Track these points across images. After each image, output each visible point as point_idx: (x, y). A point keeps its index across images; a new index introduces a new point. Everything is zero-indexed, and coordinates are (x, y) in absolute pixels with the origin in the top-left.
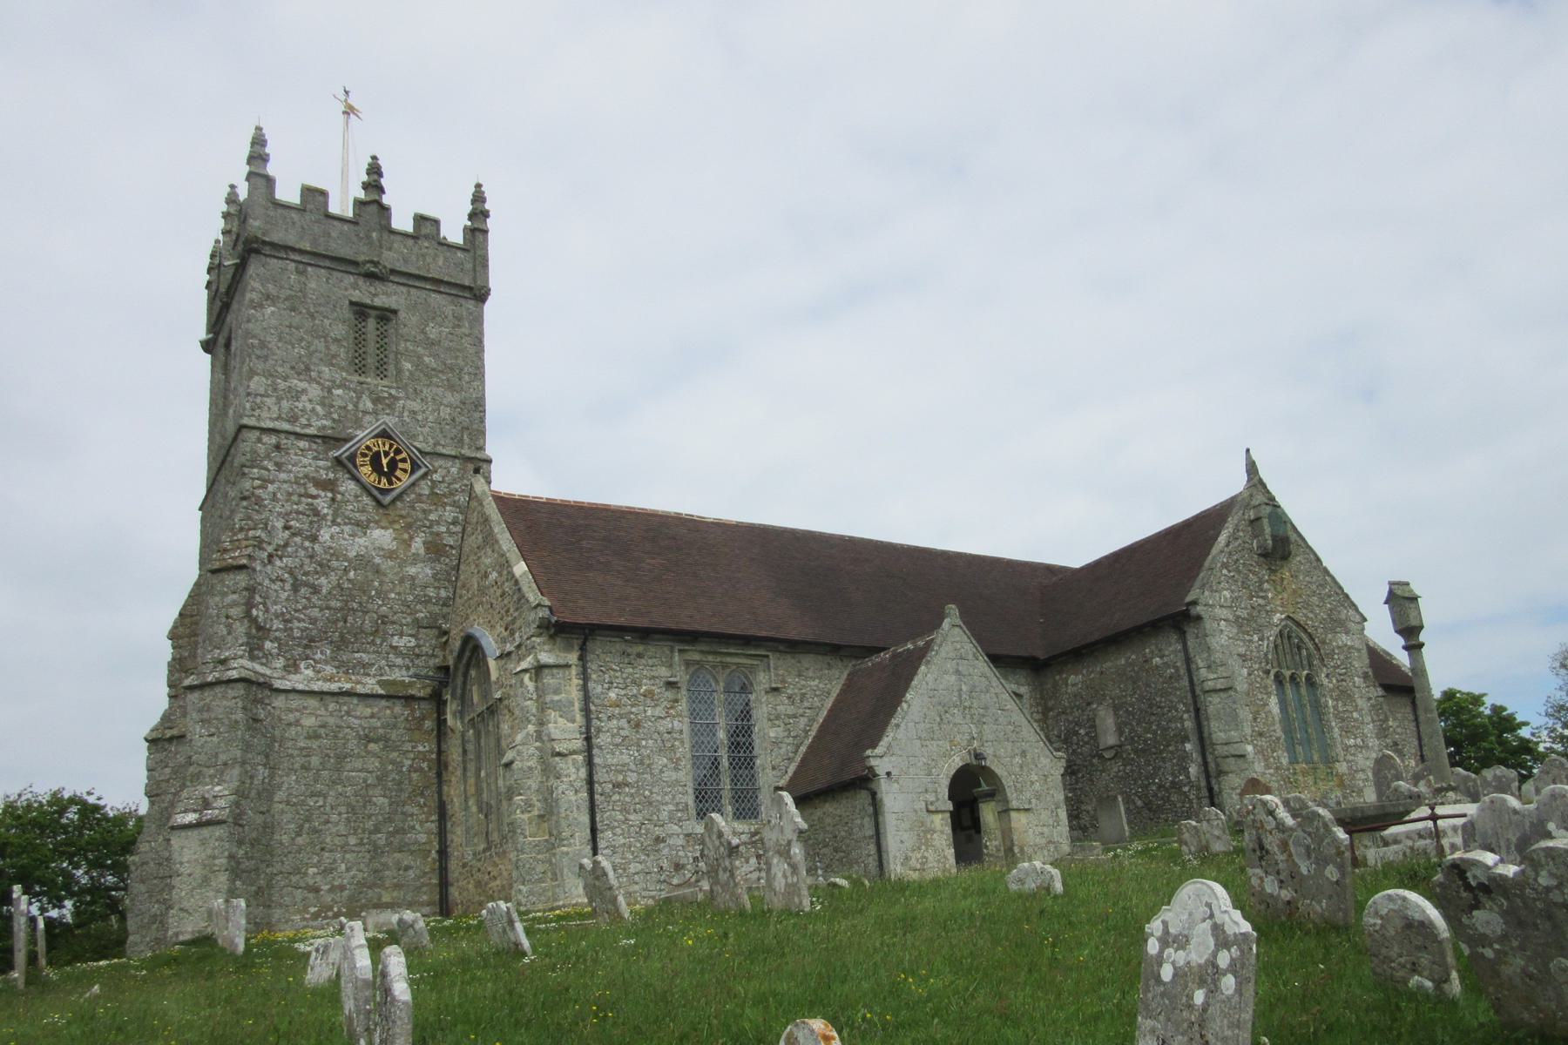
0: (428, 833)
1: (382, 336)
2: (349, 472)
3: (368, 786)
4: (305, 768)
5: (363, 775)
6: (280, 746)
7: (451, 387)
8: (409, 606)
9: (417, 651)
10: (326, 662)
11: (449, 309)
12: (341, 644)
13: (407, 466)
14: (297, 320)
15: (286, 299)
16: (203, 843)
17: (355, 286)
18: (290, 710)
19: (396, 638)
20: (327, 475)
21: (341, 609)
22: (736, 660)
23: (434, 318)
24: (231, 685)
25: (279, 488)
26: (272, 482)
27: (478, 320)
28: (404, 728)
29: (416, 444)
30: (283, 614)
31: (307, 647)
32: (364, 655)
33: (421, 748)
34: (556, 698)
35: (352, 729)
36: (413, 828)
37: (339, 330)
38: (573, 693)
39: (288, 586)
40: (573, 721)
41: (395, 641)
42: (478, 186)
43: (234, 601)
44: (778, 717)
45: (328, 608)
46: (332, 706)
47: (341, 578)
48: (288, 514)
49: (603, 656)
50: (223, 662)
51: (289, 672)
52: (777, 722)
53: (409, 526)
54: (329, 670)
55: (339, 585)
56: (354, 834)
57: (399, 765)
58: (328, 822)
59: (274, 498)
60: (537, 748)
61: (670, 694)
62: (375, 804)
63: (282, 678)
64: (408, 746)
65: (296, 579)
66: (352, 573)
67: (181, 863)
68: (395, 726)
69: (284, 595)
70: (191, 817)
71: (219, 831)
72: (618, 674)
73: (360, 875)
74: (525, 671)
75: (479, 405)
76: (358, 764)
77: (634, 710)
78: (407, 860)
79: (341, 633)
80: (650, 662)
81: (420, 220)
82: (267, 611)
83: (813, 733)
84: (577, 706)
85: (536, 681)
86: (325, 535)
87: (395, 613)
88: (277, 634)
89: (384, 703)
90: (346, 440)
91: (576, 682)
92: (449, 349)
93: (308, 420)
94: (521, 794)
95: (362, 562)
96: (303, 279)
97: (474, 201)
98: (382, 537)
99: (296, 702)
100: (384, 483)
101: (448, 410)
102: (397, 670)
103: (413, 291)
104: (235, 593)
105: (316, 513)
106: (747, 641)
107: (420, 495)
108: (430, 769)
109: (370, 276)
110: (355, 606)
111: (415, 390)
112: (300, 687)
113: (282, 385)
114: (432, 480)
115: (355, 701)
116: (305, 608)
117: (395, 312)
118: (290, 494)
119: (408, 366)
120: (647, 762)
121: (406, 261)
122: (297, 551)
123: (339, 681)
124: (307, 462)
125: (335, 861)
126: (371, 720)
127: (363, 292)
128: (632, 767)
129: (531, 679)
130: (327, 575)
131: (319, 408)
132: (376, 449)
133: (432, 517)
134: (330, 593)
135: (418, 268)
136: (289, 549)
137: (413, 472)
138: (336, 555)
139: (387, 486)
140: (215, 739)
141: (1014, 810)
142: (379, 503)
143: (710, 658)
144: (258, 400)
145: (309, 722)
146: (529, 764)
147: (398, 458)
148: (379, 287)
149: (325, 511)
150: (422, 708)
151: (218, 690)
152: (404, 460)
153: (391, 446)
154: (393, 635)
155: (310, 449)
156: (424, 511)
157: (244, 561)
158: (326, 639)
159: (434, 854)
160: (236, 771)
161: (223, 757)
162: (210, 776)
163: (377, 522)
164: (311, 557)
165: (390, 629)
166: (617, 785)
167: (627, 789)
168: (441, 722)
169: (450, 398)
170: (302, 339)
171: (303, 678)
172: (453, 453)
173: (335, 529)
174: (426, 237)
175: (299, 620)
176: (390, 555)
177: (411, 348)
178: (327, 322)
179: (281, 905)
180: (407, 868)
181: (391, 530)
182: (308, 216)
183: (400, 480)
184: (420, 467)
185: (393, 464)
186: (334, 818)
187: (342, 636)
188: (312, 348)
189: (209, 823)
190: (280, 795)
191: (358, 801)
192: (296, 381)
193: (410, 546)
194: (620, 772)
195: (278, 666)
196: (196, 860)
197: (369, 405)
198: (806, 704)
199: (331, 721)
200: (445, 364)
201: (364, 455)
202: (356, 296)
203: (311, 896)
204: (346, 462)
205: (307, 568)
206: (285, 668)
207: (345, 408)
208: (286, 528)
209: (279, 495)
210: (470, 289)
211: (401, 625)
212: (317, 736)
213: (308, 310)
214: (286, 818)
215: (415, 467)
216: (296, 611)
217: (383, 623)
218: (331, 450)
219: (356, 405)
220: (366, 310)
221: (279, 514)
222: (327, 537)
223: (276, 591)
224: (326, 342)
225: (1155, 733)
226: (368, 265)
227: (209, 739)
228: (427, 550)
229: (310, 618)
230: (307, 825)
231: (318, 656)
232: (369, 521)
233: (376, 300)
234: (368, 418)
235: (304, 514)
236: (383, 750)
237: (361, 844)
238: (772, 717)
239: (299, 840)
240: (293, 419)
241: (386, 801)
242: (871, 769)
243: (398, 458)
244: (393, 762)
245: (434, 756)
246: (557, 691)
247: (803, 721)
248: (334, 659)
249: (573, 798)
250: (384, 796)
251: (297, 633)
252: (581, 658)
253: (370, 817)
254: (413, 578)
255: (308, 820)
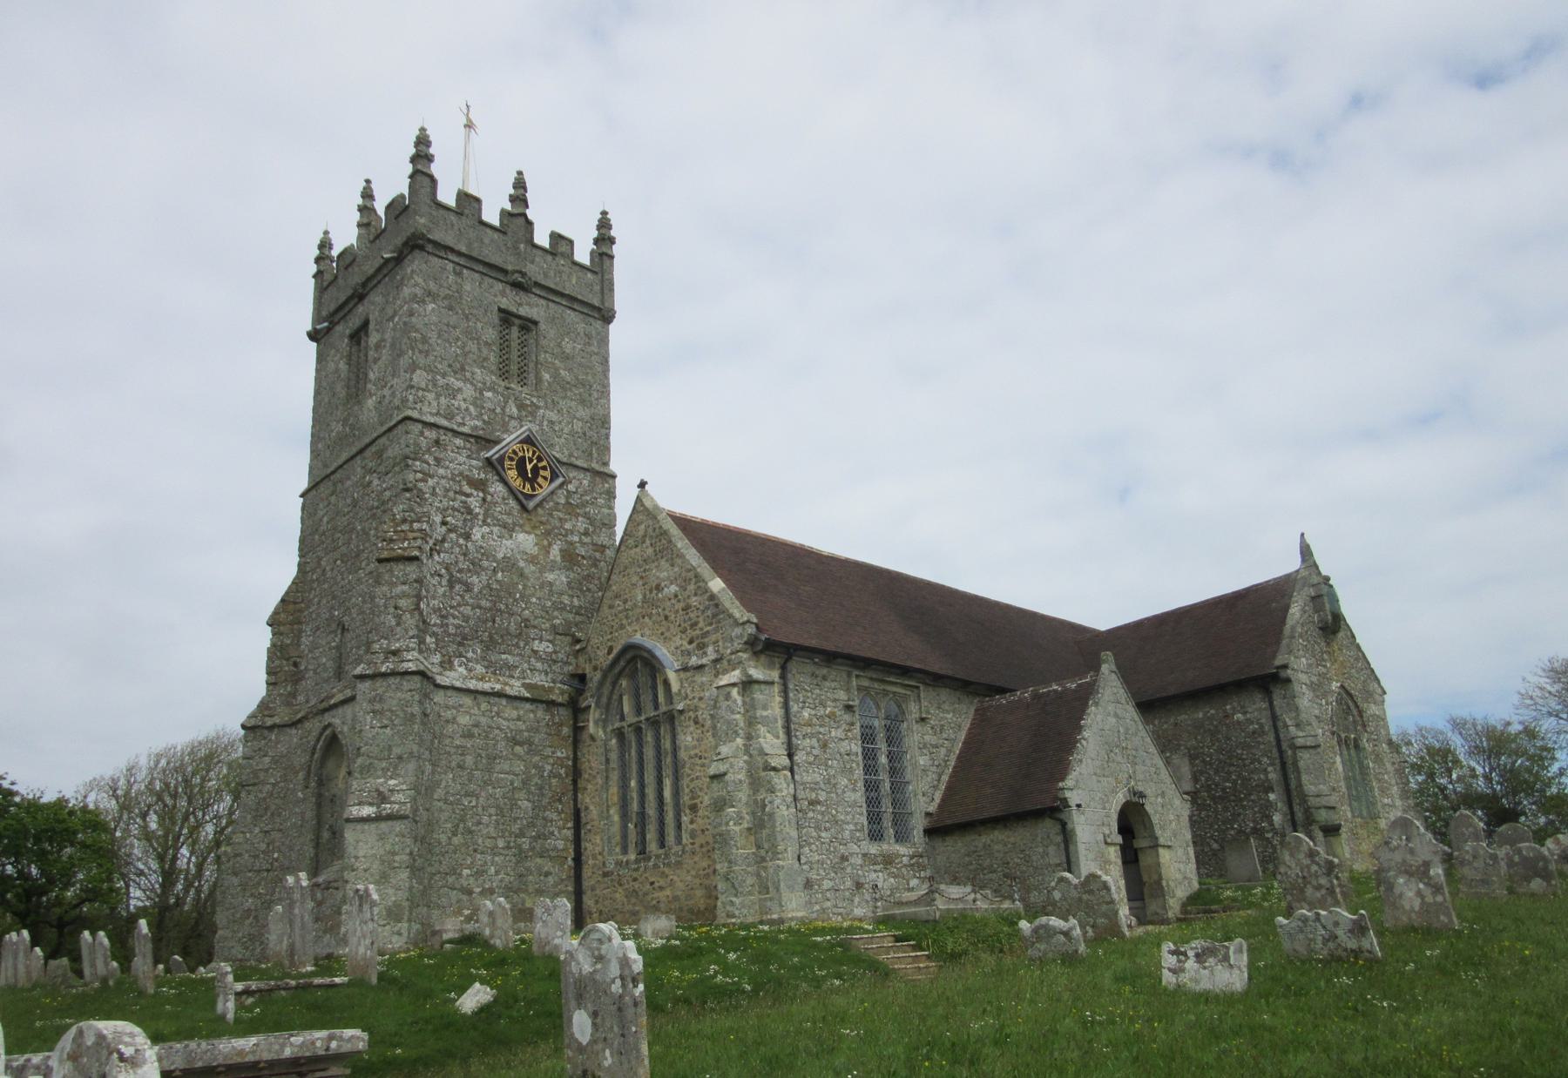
0: (566, 839)
1: (523, 344)
2: (498, 474)
3: (514, 788)
4: (460, 767)
5: (511, 777)
6: (439, 742)
7: (582, 402)
8: (547, 612)
9: (554, 656)
10: (477, 662)
11: (581, 327)
12: (490, 645)
13: (547, 474)
14: (453, 320)
15: (445, 298)
16: (381, 837)
17: (503, 294)
18: (448, 707)
19: (537, 642)
20: (479, 474)
21: (490, 609)
22: (894, 689)
23: (569, 333)
24: (408, 677)
25: (438, 483)
26: (432, 477)
27: (604, 341)
28: (546, 733)
29: (554, 453)
30: (440, 609)
31: (460, 644)
32: (509, 657)
33: (559, 754)
34: (765, 713)
35: (501, 730)
36: (552, 833)
37: (491, 334)
38: (776, 710)
39: (444, 582)
40: (778, 737)
41: (536, 645)
42: (604, 213)
43: (404, 592)
44: (925, 746)
45: (480, 608)
46: (484, 706)
47: (490, 578)
48: (446, 510)
49: (798, 676)
50: (395, 653)
51: (445, 669)
52: (924, 751)
53: (548, 533)
54: (480, 669)
55: (489, 586)
56: (503, 837)
57: (541, 769)
58: (479, 823)
59: (434, 494)
60: (745, 762)
61: (847, 717)
62: (520, 808)
63: (441, 674)
64: (548, 751)
65: (451, 576)
66: (500, 574)
67: (356, 858)
68: (537, 730)
69: (441, 591)
70: (367, 811)
71: (399, 826)
72: (809, 694)
73: (507, 878)
74: (734, 685)
75: (605, 422)
76: (506, 767)
77: (822, 730)
78: (548, 866)
79: (490, 633)
80: (833, 685)
81: (556, 238)
82: (428, 605)
83: (952, 763)
84: (780, 723)
85: (743, 696)
86: (477, 533)
87: (536, 618)
88: (434, 629)
89: (528, 706)
90: (497, 442)
91: (778, 699)
92: (580, 365)
93: (463, 418)
94: (733, 806)
95: (509, 564)
96: (459, 281)
97: (599, 227)
98: (525, 541)
99: (454, 699)
100: (527, 490)
101: (580, 424)
102: (537, 674)
104: (404, 583)
105: (469, 511)
106: (905, 671)
107: (558, 504)
108: (567, 775)
109: (517, 286)
110: (503, 607)
111: (553, 401)
112: (458, 684)
113: (441, 381)
114: (568, 491)
115: (504, 702)
116: (459, 605)
117: (536, 323)
118: (447, 490)
119: (546, 376)
120: (833, 781)
121: (546, 275)
122: (452, 548)
123: (489, 681)
124: (461, 460)
125: (486, 862)
126: (519, 723)
127: (509, 300)
128: (822, 786)
129: (739, 693)
130: (478, 574)
131: (472, 408)
132: (521, 454)
133: (568, 526)
134: (480, 592)
135: (556, 284)
136: (446, 545)
137: (552, 480)
138: (487, 555)
139: (530, 492)
140: (388, 731)
141: (1164, 846)
142: (524, 508)
143: (876, 686)
144: (420, 393)
145: (464, 720)
146: (739, 777)
147: (540, 465)
148: (523, 297)
149: (477, 510)
150: (564, 713)
151: (392, 680)
152: (544, 468)
153: (534, 453)
154: (534, 639)
155: (464, 448)
156: (560, 519)
157: (416, 553)
158: (477, 638)
159: (570, 862)
160: (412, 766)
161: (397, 751)
162: (383, 769)
163: (521, 526)
164: (465, 555)
165: (533, 633)
166: (812, 803)
167: (819, 807)
168: (577, 730)
169: (582, 413)
170: (458, 339)
171: (455, 676)
172: (585, 466)
173: (486, 529)
174: (562, 255)
175: (454, 617)
176: (532, 560)
178: (479, 325)
179: (439, 906)
180: (547, 874)
181: (533, 536)
183: (541, 487)
184: (558, 476)
185: (536, 470)
186: (485, 819)
187: (491, 637)
188: (467, 349)
189: (390, 817)
190: (439, 793)
191: (505, 804)
192: (452, 379)
193: (549, 552)
194: (812, 790)
195: (435, 661)
196: (374, 855)
197: (515, 410)
198: (945, 736)
199: (483, 720)
200: (577, 379)
201: (511, 459)
202: (505, 303)
203: (465, 898)
204: (496, 463)
205: (461, 566)
206: (441, 664)
207: (494, 410)
208: (444, 523)
209: (437, 490)
210: (599, 310)
211: (541, 630)
212: (470, 735)
213: (463, 310)
214: (444, 816)
215: (554, 476)
216: (452, 607)
217: (526, 626)
218: (482, 450)
219: (503, 409)
220: (513, 319)
221: (438, 508)
222: (479, 536)
223: (434, 585)
224: (478, 343)
225: (1234, 782)
226: (516, 275)
227: (381, 731)
228: (563, 557)
229: (463, 616)
230: (461, 826)
231: (470, 655)
232: (514, 524)
233: (520, 309)
234: (513, 423)
235: (459, 511)
236: (528, 753)
237: (508, 847)
238: (921, 746)
239: (456, 840)
240: (450, 416)
241: (530, 805)
242: (1065, 800)
243: (540, 465)
244: (536, 766)
245: (570, 763)
246: (765, 708)
247: (943, 751)
248: (484, 658)
249: (786, 813)
250: (528, 800)
251: (452, 630)
252: (783, 677)
253: (516, 819)
254: (551, 584)
255: (463, 819)
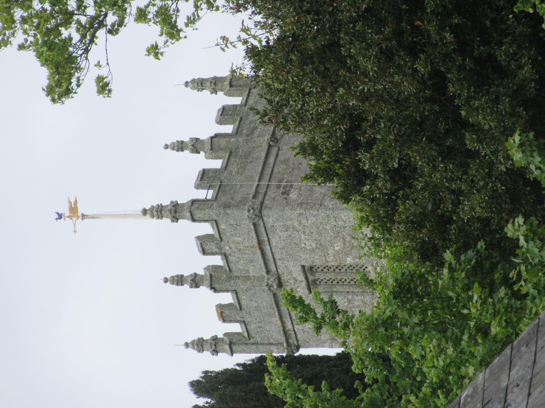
103: (277, 257)
117: (303, 267)
177: (332, 258)
182: (247, 319)
